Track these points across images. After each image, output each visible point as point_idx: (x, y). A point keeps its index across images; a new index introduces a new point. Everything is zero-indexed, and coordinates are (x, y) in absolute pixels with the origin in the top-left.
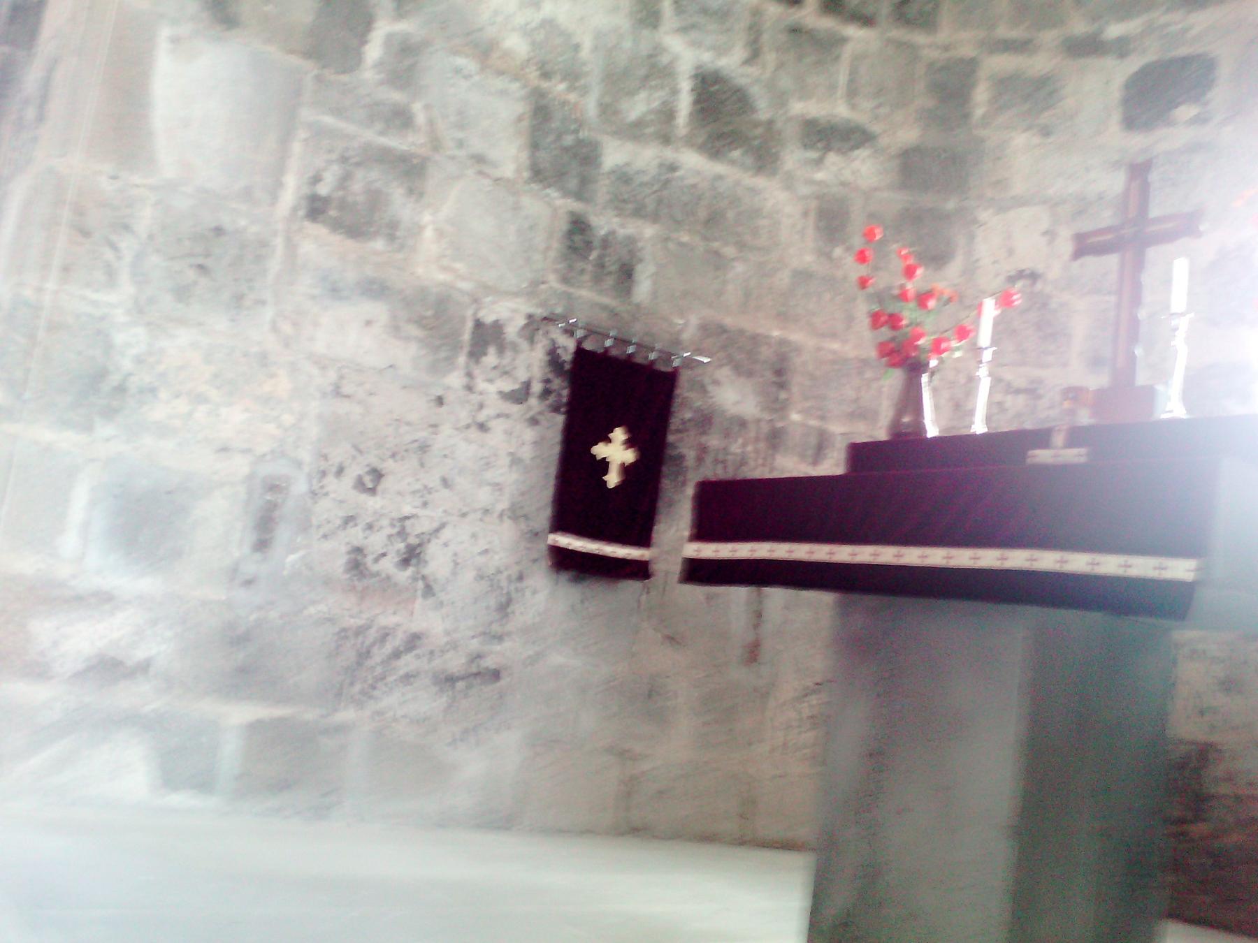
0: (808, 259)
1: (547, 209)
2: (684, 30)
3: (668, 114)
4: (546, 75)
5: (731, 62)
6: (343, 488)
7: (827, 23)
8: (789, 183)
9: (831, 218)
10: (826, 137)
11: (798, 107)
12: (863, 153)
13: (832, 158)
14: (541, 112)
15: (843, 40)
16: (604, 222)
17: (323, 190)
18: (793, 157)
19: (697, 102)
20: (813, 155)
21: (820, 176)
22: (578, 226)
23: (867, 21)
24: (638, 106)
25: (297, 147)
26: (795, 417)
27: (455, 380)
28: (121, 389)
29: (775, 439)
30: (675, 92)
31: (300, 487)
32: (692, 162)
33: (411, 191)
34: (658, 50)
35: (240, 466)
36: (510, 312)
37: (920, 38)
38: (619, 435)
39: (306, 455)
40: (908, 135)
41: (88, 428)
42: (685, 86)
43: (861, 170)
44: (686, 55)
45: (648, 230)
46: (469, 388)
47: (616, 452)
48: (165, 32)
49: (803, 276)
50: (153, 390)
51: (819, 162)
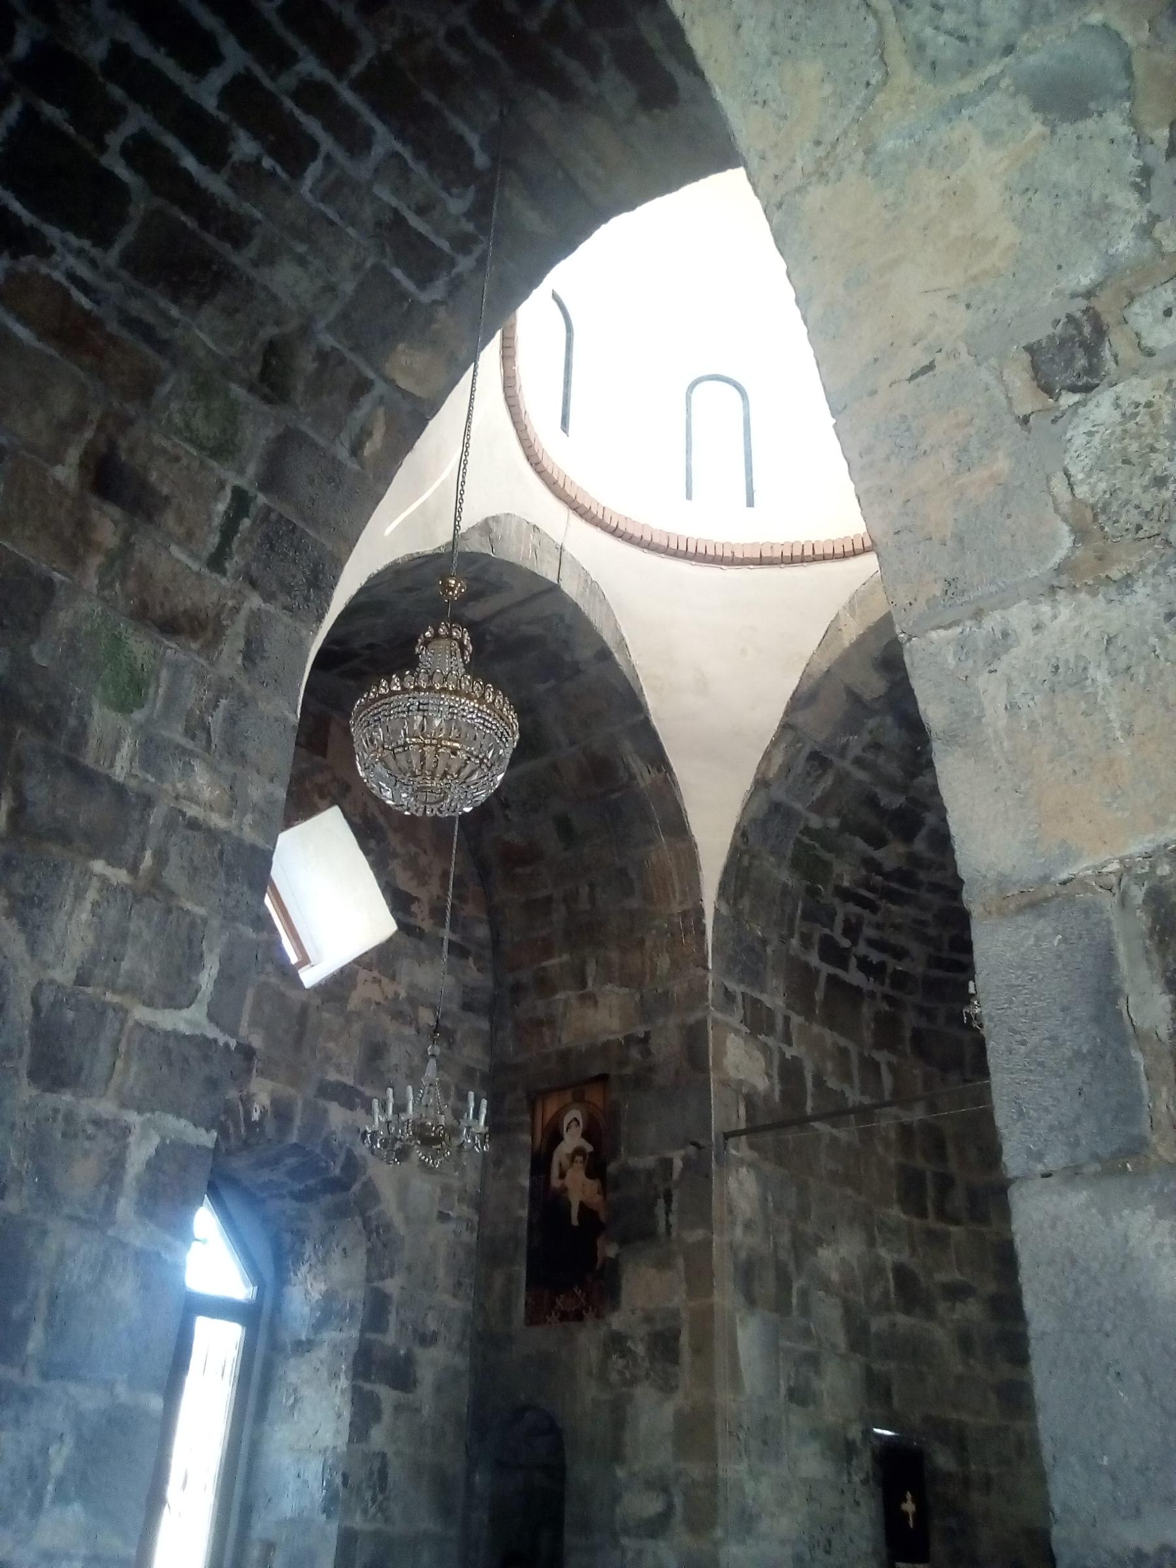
0: (957, 1367)
1: (856, 1365)
2: (884, 1244)
3: (886, 1293)
4: (846, 1289)
5: (905, 1257)
6: (820, 1553)
7: (939, 1226)
8: (942, 1324)
9: (965, 1341)
10: (956, 1292)
11: (941, 1277)
12: (971, 1300)
13: (959, 1305)
14: (849, 1312)
15: (948, 1235)
16: (876, 1366)
17: (792, 1384)
18: (942, 1307)
19: (897, 1284)
20: (949, 1304)
21: (955, 1317)
22: (868, 1370)
23: (957, 1222)
24: (876, 1294)
25: (781, 1363)
26: (973, 1467)
27: (845, 1479)
28: (751, 1516)
29: (966, 1482)
30: (888, 1279)
31: (808, 1557)
32: (901, 1319)
33: (816, 1372)
34: (878, 1257)
35: (788, 1551)
36: (855, 1432)
37: (984, 1229)
38: (909, 1495)
39: (806, 1538)
40: (991, 1287)
41: (742, 1542)
42: (891, 1276)
43: (972, 1310)
44: (888, 1257)
45: (892, 1366)
46: (850, 1481)
47: (909, 1507)
48: (738, 1317)
49: (960, 1379)
50: (759, 1516)
51: (952, 1309)
